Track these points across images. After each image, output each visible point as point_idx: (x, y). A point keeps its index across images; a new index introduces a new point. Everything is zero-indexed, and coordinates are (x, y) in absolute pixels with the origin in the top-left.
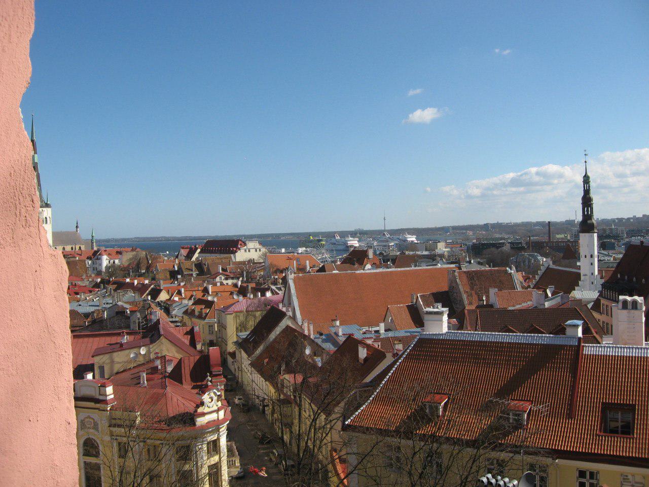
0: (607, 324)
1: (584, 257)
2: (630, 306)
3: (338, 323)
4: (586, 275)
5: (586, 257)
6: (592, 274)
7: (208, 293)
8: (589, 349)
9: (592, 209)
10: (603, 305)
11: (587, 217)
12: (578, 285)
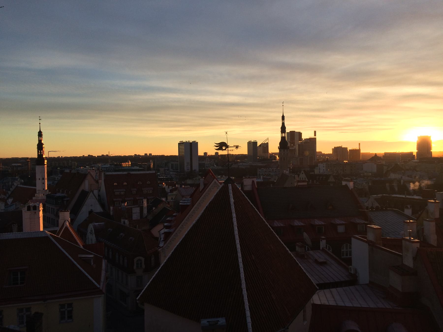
1: (38, 179)
2: (32, 209)
4: (40, 190)
5: (39, 179)
6: (44, 189)
10: (47, 207)
11: (40, 156)
12: (34, 196)
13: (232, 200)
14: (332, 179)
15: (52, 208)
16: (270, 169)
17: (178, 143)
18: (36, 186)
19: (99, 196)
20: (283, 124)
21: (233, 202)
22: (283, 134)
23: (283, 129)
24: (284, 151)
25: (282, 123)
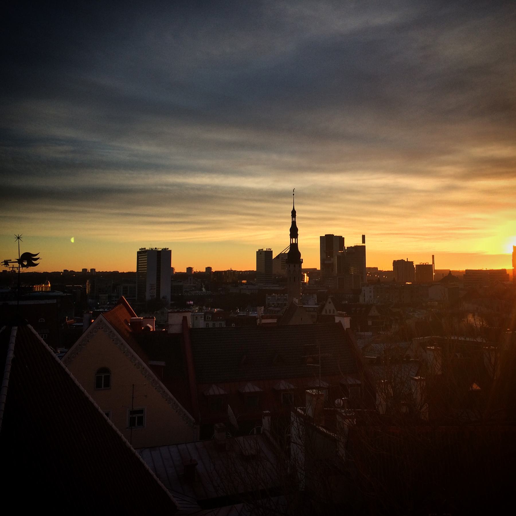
13: (11, 355)
14: (374, 312)
16: (286, 295)
17: (138, 252)
20: (294, 223)
21: (11, 359)
22: (294, 239)
23: (294, 232)
24: (295, 266)
25: (291, 221)
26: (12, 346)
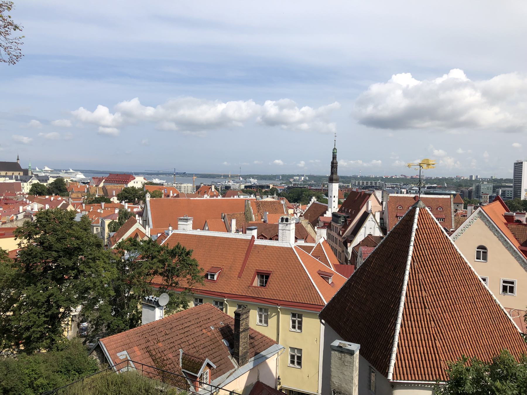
0: (333, 236)
3: (170, 228)
6: (334, 207)
7: (102, 207)
8: (258, 242)
9: (337, 168)
12: (326, 214)
13: (415, 227)
15: (336, 227)
18: (327, 204)
19: (381, 219)
26: (416, 221)
